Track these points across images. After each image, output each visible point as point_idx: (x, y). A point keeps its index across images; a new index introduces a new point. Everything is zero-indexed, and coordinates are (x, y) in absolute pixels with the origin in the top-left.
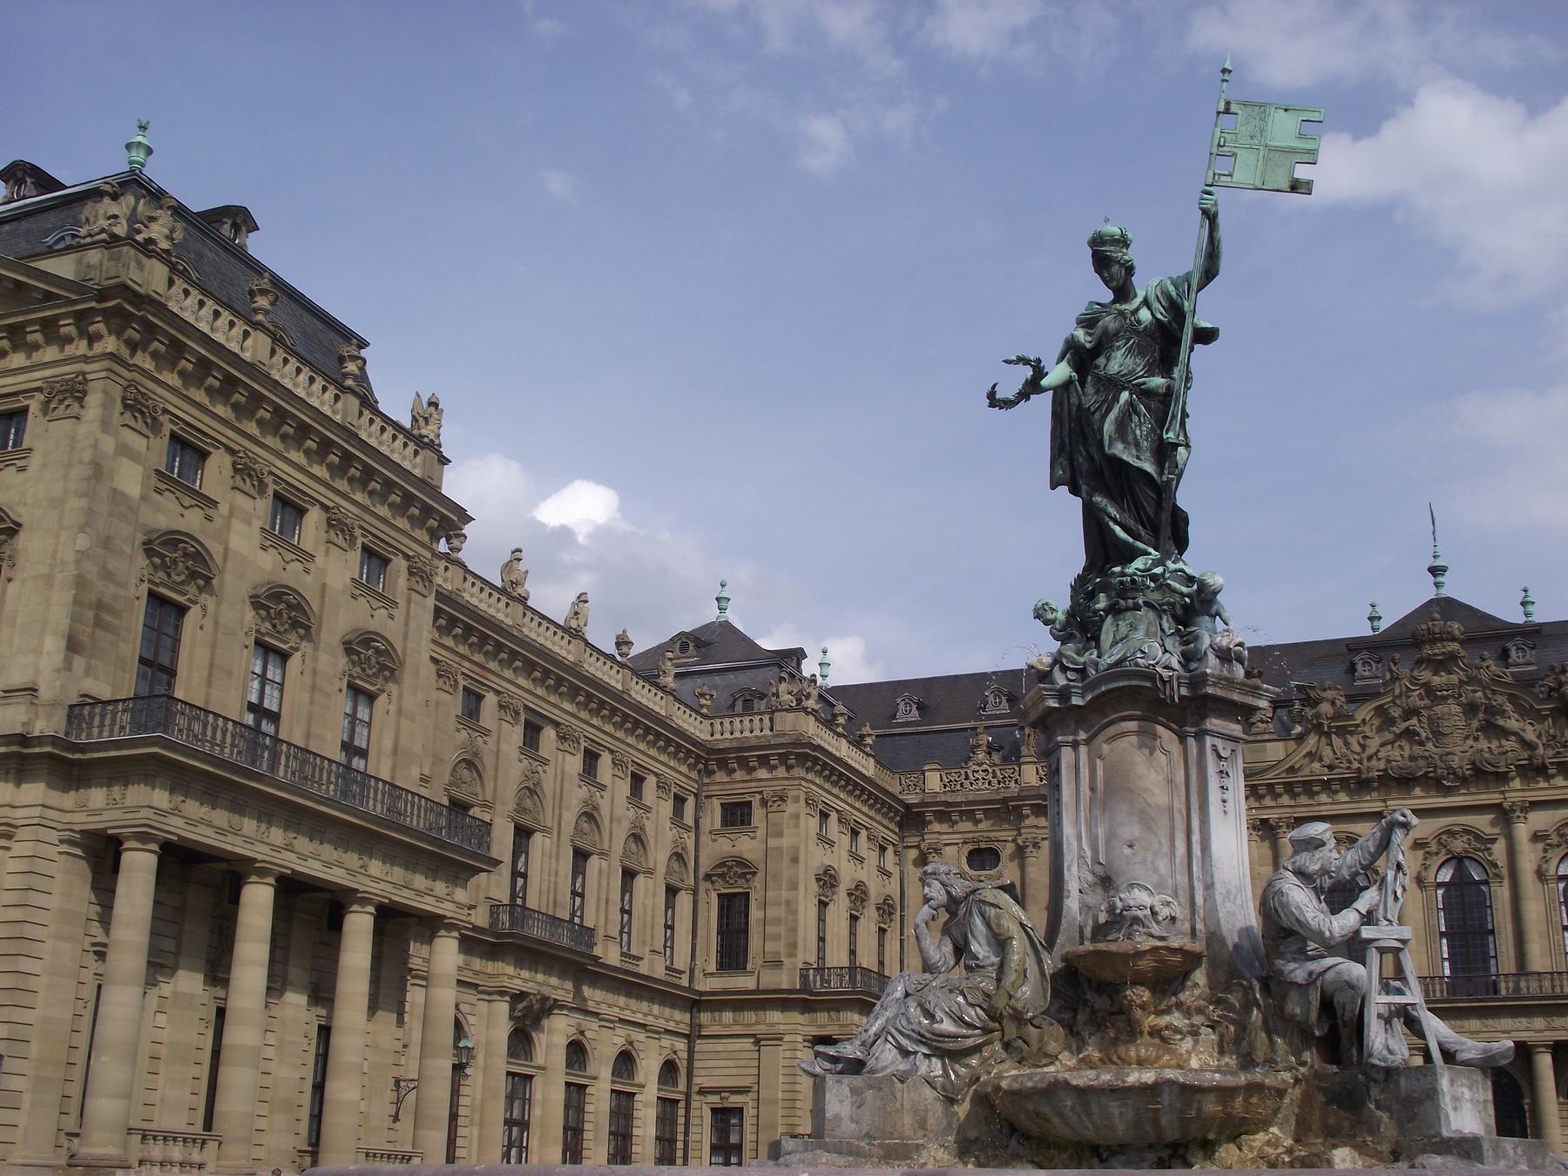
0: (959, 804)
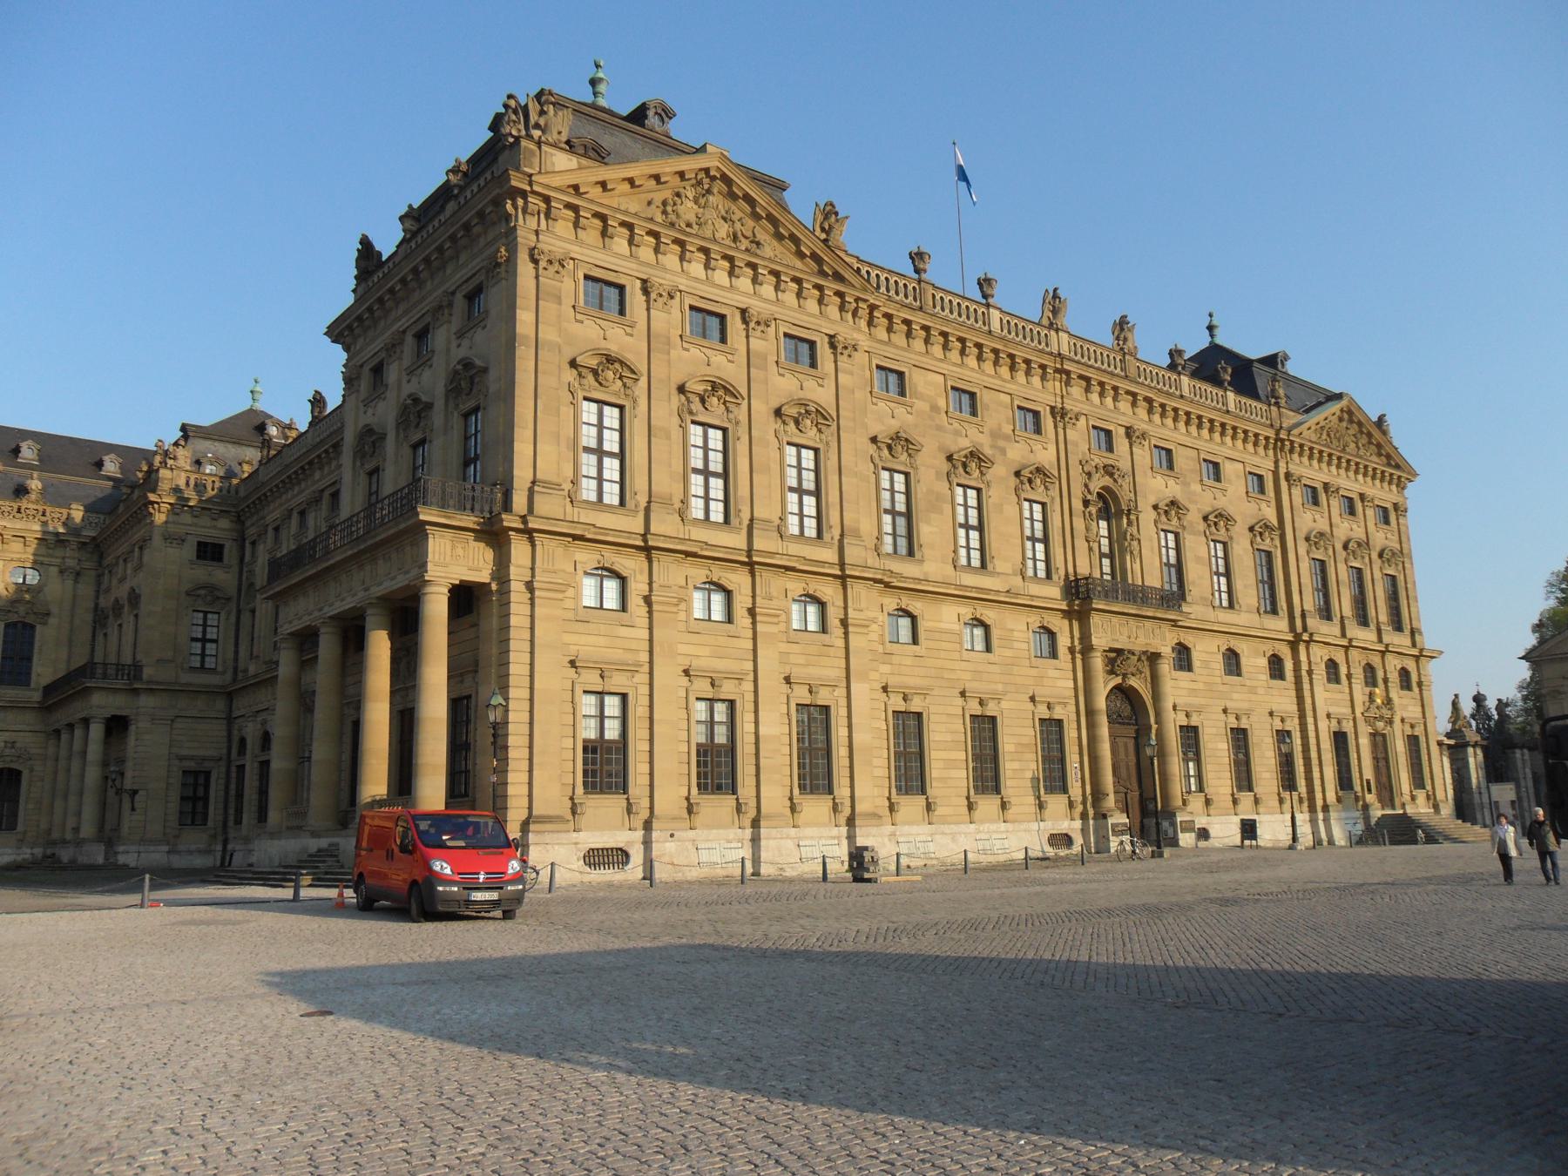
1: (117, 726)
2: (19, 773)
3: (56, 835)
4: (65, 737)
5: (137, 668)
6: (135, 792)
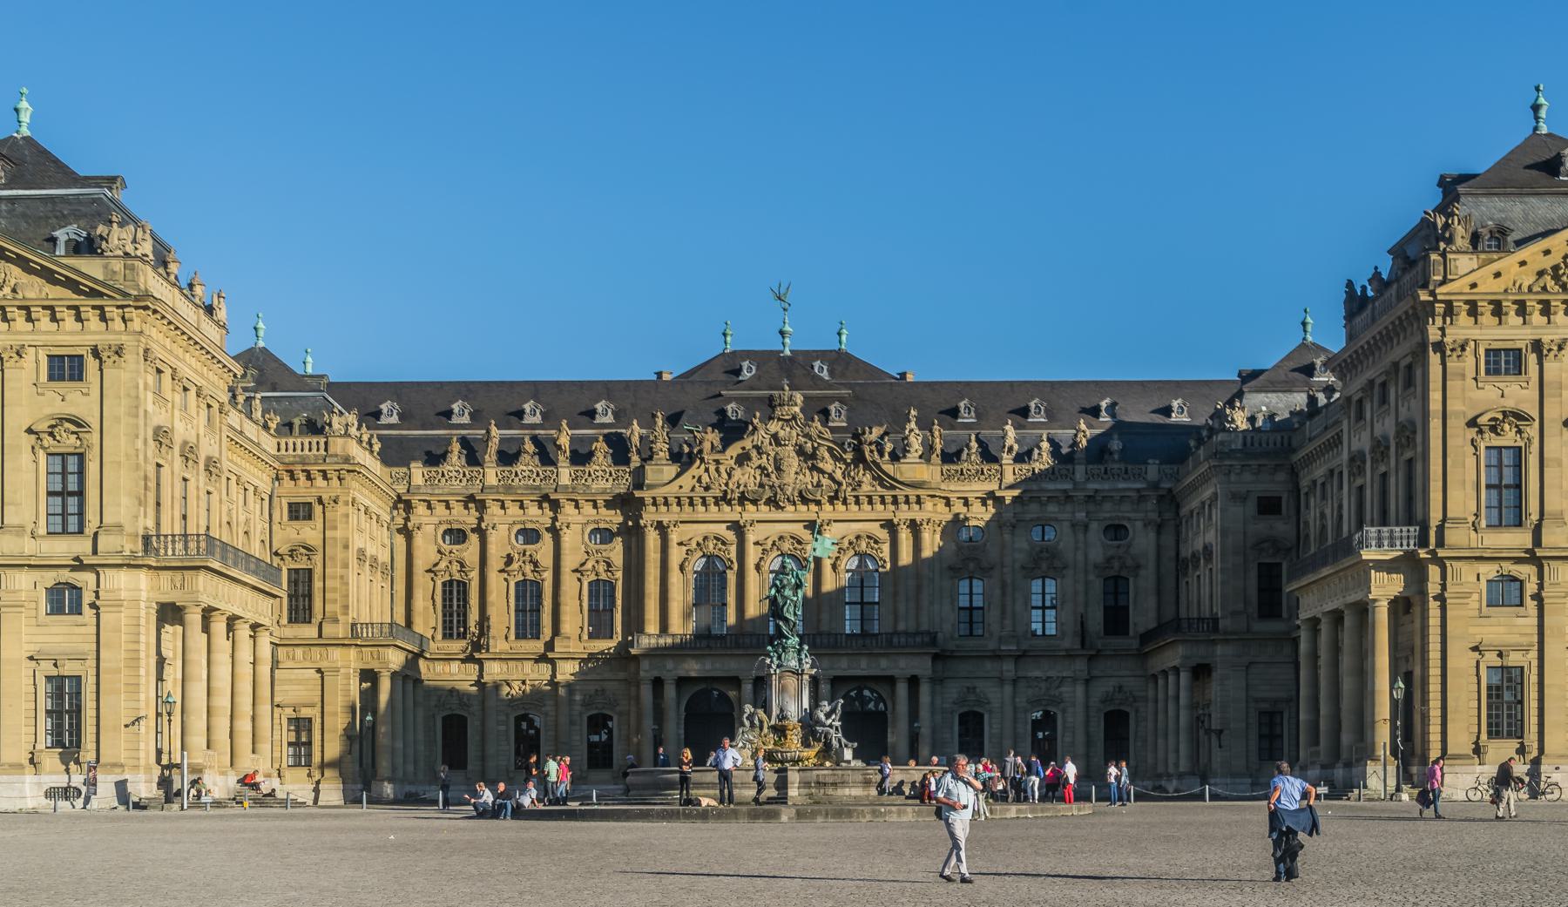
1: (1201, 672)
2: (1127, 714)
3: (1160, 769)
4: (1161, 682)
5: (1215, 620)
6: (1221, 731)
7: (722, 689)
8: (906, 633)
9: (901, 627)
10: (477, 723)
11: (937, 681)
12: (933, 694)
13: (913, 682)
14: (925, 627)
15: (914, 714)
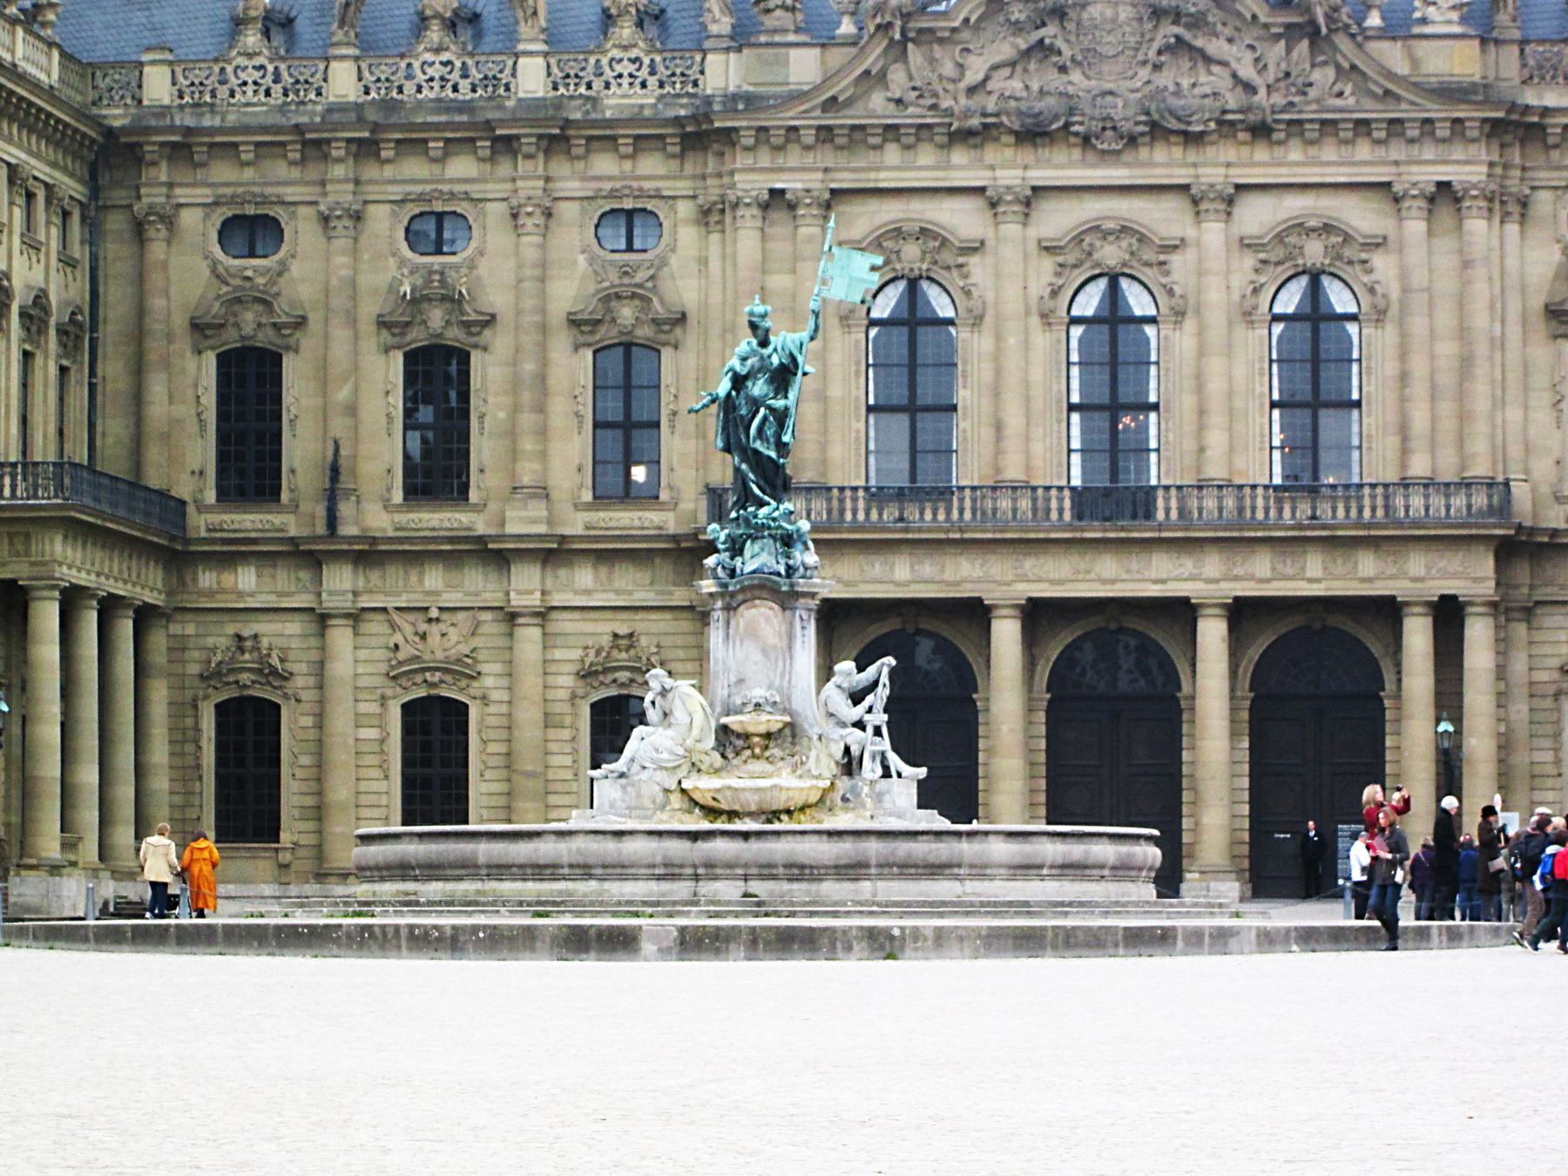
0: (212, 131)
7: (946, 632)
8: (1428, 484)
9: (1419, 467)
10: (308, 721)
11: (1511, 610)
12: (1503, 647)
13: (1448, 615)
14: (1480, 469)
15: (1449, 699)
